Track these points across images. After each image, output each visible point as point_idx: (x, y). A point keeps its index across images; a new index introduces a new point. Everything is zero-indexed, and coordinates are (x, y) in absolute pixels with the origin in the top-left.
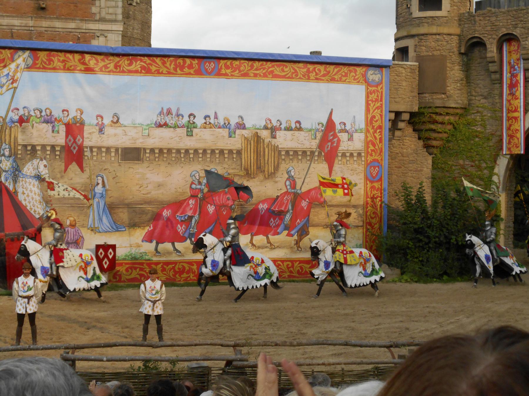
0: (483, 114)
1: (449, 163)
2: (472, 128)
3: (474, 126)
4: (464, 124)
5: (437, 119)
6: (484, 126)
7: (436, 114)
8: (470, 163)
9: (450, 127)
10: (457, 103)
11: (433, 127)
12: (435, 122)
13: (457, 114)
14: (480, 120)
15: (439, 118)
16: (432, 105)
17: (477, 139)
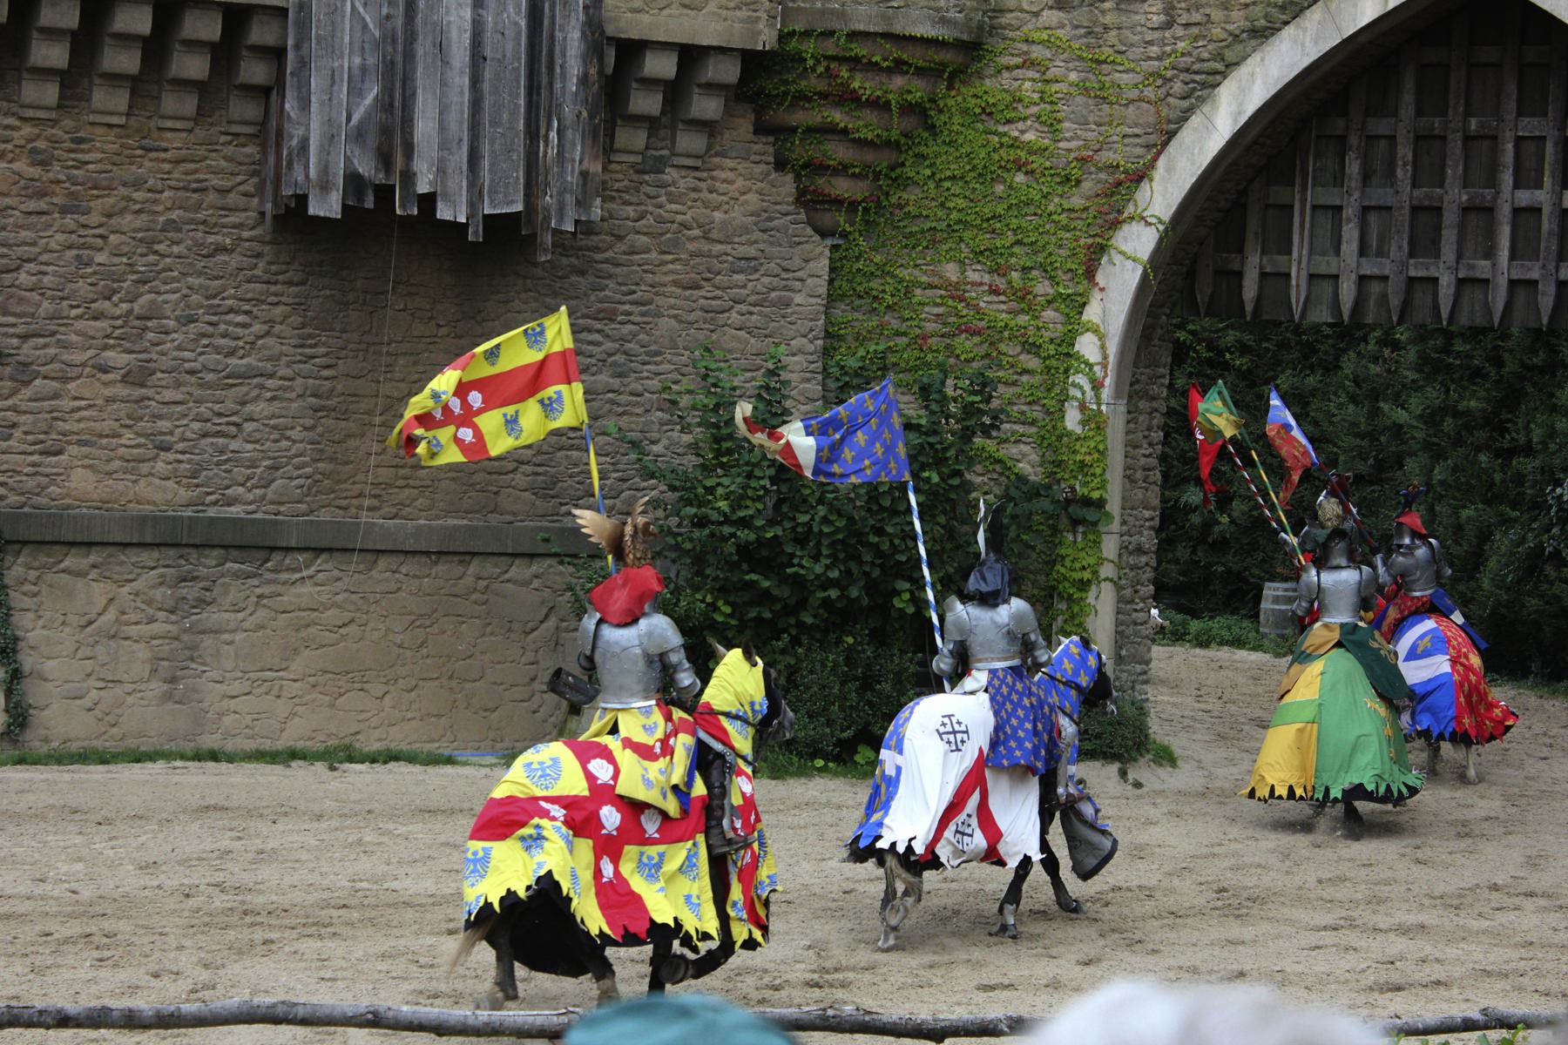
0: (1049, 75)
1: (903, 273)
2: (1001, 129)
3: (1009, 122)
4: (965, 112)
5: (856, 85)
6: (1052, 126)
7: (855, 63)
8: (987, 278)
9: (909, 123)
10: (944, 21)
11: (838, 116)
12: (849, 99)
13: (944, 65)
14: (1036, 96)
15: (861, 83)
16: (836, 25)
17: (1020, 178)
